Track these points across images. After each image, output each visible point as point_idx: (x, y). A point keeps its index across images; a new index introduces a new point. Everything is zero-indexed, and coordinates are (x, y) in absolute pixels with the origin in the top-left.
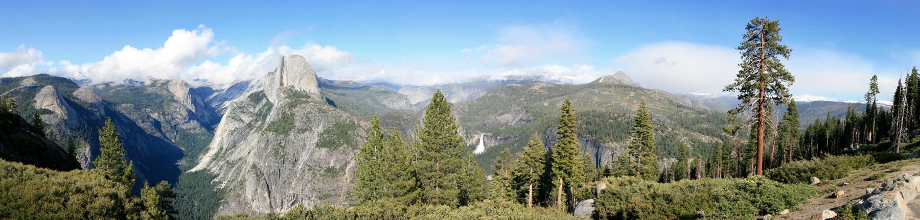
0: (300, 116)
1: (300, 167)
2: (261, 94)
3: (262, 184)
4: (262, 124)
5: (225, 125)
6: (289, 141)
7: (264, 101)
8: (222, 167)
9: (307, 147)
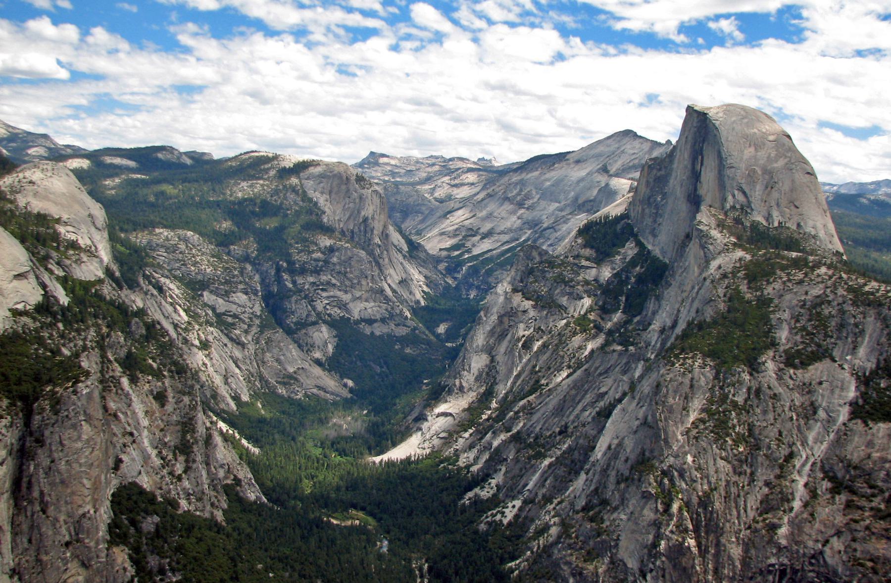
1: (801, 481)
2: (619, 227)
3: (677, 527)
4: (627, 322)
5: (501, 317)
6: (758, 392)
7: (630, 250)
8: (498, 449)
9: (821, 414)
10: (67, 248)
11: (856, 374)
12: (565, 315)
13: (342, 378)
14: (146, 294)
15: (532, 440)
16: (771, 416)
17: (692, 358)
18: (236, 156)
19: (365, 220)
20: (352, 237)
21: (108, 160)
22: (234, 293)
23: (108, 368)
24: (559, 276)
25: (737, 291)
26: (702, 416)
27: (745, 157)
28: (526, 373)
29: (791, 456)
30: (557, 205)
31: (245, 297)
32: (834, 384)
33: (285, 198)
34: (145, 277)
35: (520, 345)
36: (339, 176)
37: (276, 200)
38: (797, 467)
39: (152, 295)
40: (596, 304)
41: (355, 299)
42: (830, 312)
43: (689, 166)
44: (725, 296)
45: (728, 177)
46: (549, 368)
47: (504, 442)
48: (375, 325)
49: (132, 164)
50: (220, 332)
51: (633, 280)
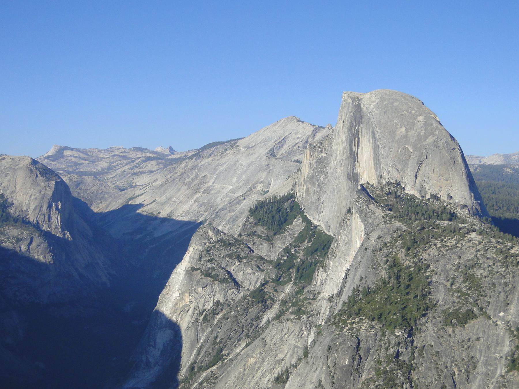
2: (286, 205)
4: (300, 292)
5: (182, 294)
9: (481, 368)
11: (510, 329)
17: (358, 322)
24: (235, 252)
27: (397, 137)
28: (208, 344)
35: (201, 318)
40: (269, 277)
42: (481, 274)
43: (348, 147)
51: (302, 253)
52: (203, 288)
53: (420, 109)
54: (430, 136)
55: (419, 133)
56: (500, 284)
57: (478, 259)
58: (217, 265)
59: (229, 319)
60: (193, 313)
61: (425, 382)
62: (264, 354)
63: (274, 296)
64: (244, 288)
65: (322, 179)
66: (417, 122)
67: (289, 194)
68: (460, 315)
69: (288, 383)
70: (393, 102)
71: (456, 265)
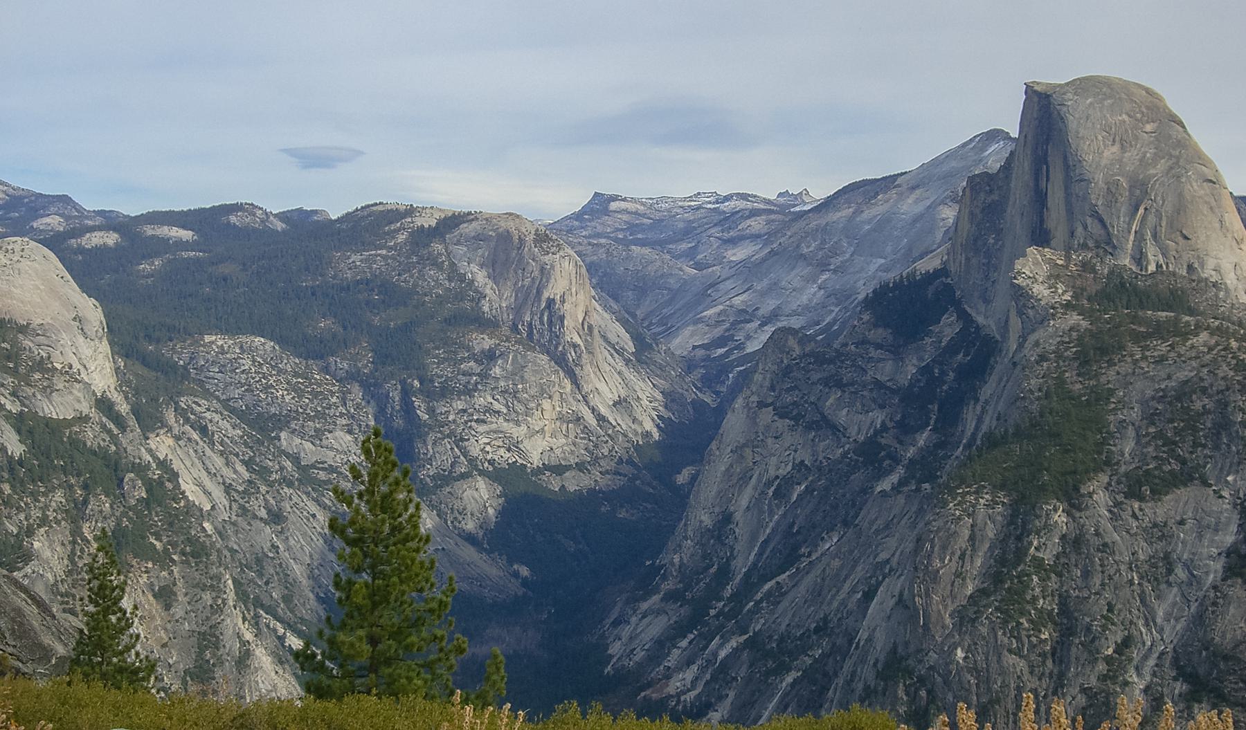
0: (1144, 403)
7: (948, 327)
9: (1180, 573)
10: (32, 369)
12: (843, 440)
13: (510, 562)
14: (177, 438)
15: (774, 645)
16: (1097, 581)
17: (976, 492)
18: (348, 214)
19: (551, 302)
20: (530, 334)
21: (149, 231)
22: (330, 432)
23: (82, 551)
25: (1061, 382)
26: (986, 585)
29: (1126, 643)
30: (883, 261)
31: (349, 438)
32: (1205, 523)
33: (422, 276)
34: (182, 413)
36: (505, 237)
37: (406, 281)
38: (1135, 663)
39: (189, 439)
40: (891, 420)
41: (532, 434)
42: (1204, 407)
43: (1032, 184)
44: (1040, 390)
45: (1077, 196)
46: (814, 526)
47: (736, 651)
48: (567, 474)
49: (186, 235)
50: (304, 497)
52: (776, 438)
53: (1153, 110)
54: (1164, 158)
55: (1145, 153)
56: (1235, 423)
57: (1202, 379)
58: (802, 398)
59: (816, 493)
60: (759, 480)
61: (1078, 597)
62: (856, 551)
63: (896, 451)
64: (849, 438)
65: (991, 241)
66: (1145, 135)
67: (936, 271)
68: (1157, 481)
69: (875, 600)
70: (1104, 100)
71: (1163, 390)
